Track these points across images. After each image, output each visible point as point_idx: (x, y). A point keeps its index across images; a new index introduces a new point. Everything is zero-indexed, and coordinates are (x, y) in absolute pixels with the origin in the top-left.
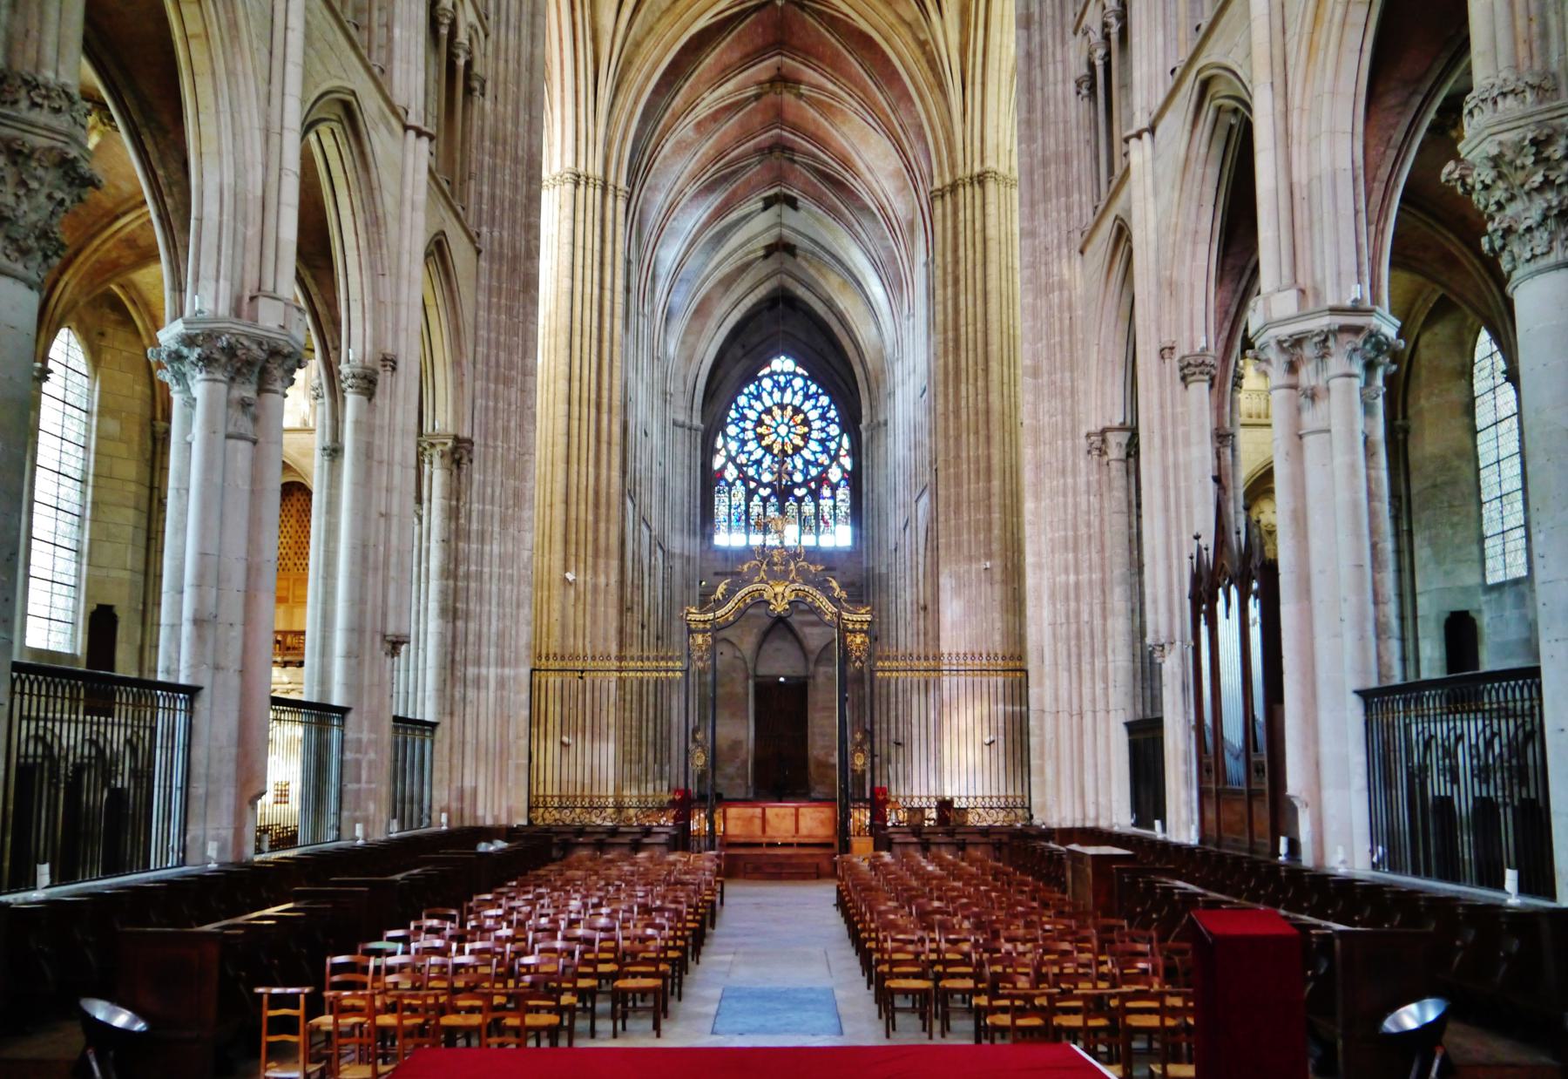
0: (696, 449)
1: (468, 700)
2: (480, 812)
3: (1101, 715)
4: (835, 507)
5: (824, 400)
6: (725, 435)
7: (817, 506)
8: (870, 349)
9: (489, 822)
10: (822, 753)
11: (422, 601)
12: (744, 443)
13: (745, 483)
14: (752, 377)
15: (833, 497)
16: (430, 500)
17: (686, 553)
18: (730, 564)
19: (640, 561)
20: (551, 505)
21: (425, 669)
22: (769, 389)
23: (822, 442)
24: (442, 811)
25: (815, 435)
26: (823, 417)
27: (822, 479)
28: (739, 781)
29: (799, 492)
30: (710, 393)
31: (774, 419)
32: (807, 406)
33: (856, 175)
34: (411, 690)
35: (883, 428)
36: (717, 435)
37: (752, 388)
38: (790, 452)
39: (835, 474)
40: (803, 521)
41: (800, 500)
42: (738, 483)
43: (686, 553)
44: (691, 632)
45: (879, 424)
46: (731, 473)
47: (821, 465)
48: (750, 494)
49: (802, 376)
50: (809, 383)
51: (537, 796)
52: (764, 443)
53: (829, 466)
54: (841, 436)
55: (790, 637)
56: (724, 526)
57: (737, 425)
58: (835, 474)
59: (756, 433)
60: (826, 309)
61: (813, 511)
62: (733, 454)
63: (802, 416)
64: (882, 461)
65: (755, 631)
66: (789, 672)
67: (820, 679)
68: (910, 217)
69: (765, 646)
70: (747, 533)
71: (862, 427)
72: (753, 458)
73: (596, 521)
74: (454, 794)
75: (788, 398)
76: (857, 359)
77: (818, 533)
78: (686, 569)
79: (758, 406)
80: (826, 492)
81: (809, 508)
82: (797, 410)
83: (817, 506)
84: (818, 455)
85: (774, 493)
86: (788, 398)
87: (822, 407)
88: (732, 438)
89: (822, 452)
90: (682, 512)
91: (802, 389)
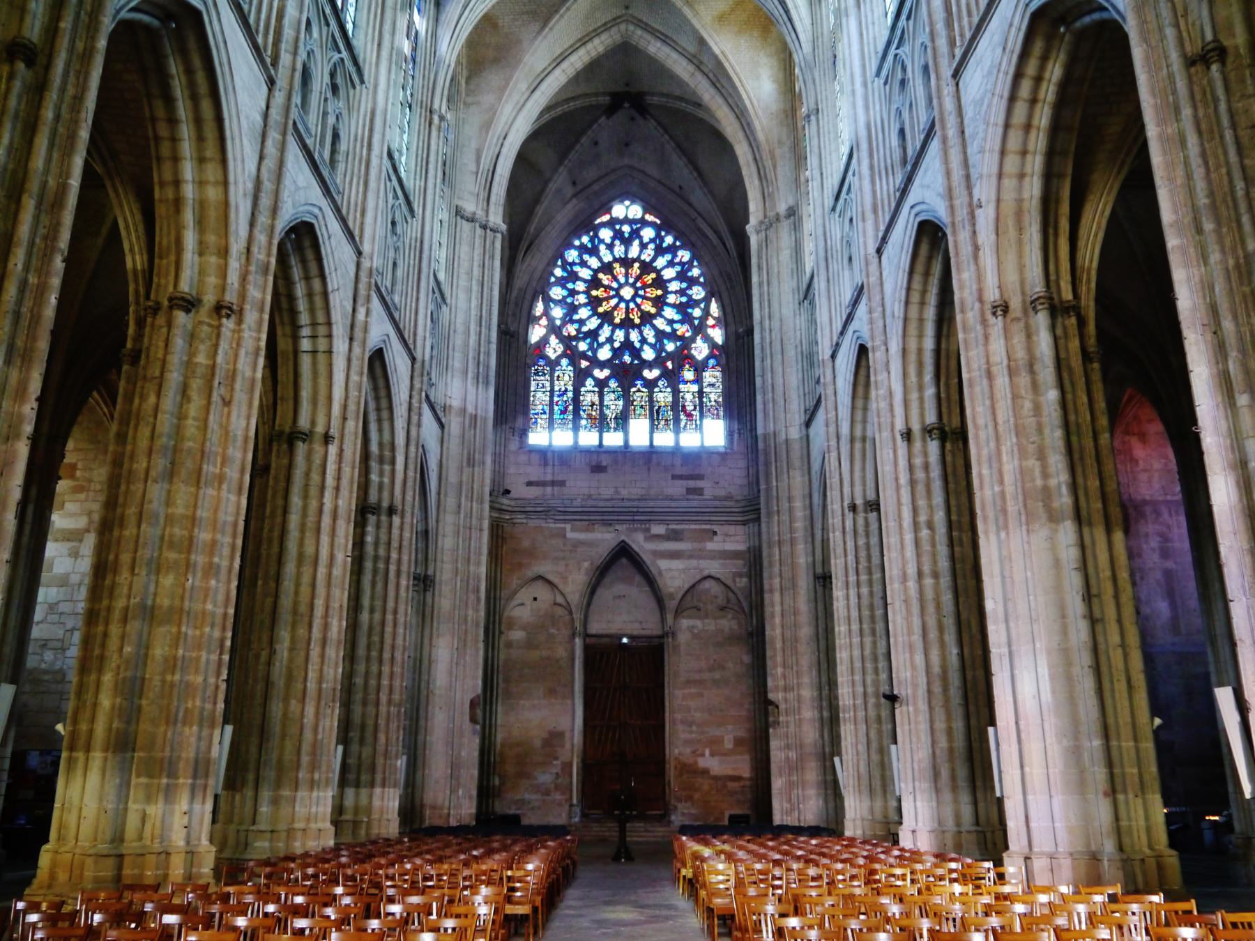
0: (492, 257)
4: (701, 393)
5: (684, 255)
6: (548, 300)
7: (676, 393)
8: (760, 113)
10: (688, 750)
12: (573, 309)
13: (574, 363)
14: (587, 225)
15: (698, 380)
22: (608, 241)
23: (681, 308)
25: (671, 299)
26: (681, 276)
27: (683, 357)
28: (558, 796)
31: (615, 278)
32: (661, 262)
37: (585, 239)
38: (637, 321)
39: (700, 350)
40: (655, 416)
41: (651, 385)
42: (564, 362)
43: (470, 409)
46: (554, 348)
47: (682, 338)
48: (580, 377)
52: (601, 310)
53: (693, 339)
54: (707, 300)
55: (638, 578)
56: (542, 421)
57: (564, 287)
58: (700, 350)
60: (691, 68)
61: (670, 399)
62: (558, 323)
63: (653, 275)
65: (586, 565)
66: (636, 630)
67: (683, 638)
69: (599, 592)
70: (576, 428)
71: (750, 229)
72: (585, 329)
75: (634, 251)
76: (741, 134)
77: (677, 431)
78: (469, 434)
79: (594, 263)
80: (689, 374)
81: (663, 396)
82: (647, 267)
83: (676, 393)
84: (676, 326)
86: (634, 251)
87: (681, 264)
88: (557, 302)
89: (682, 322)
90: (466, 345)
91: (652, 241)
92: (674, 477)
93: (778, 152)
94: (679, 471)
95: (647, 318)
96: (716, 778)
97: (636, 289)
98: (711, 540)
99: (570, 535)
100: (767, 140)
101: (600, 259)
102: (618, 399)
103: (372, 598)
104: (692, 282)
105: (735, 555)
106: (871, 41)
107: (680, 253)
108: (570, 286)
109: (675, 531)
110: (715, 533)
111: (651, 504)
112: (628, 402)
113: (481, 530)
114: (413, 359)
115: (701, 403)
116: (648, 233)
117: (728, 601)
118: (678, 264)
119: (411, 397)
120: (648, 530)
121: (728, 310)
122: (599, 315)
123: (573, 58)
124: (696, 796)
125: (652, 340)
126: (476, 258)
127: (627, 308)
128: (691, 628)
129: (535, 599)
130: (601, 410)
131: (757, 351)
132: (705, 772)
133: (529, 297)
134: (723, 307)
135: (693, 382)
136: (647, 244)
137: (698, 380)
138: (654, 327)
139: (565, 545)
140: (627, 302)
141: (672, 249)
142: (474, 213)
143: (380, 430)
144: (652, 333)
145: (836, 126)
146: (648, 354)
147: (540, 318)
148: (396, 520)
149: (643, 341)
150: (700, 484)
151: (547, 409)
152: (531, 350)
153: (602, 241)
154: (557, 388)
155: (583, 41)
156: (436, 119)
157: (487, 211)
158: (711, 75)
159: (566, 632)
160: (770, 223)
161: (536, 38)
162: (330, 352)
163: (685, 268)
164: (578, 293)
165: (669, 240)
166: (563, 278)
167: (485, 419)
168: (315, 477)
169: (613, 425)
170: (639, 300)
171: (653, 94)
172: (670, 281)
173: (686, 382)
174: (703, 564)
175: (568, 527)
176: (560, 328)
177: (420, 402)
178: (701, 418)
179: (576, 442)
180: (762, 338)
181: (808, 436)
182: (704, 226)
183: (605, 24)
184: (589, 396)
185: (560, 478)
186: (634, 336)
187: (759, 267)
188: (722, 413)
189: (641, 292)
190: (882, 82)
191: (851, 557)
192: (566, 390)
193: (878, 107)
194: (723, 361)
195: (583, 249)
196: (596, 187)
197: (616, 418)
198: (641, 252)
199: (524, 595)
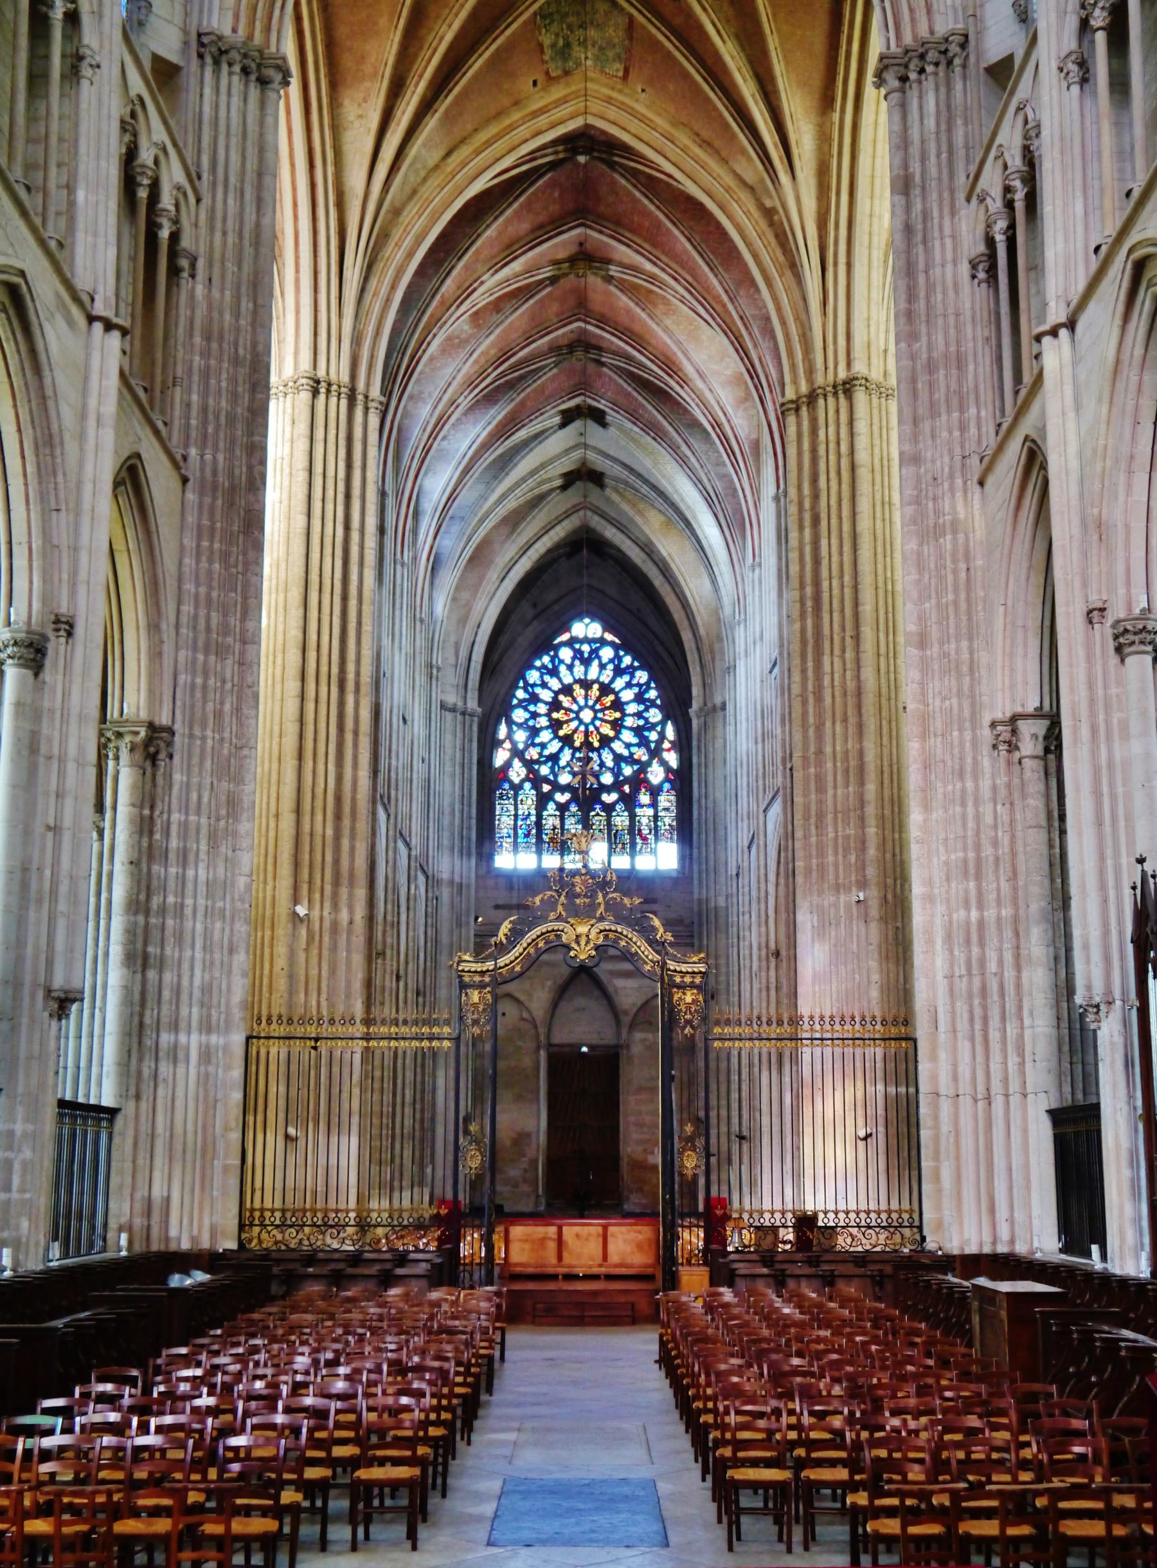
0: (471, 741)
1: (160, 1078)
2: (173, 1232)
3: (1015, 1100)
4: (656, 817)
5: (642, 676)
6: (510, 722)
7: (633, 816)
8: (702, 611)
9: (185, 1245)
10: (640, 1148)
11: (101, 944)
12: (535, 732)
13: (536, 786)
14: (546, 645)
15: (654, 804)
16: (115, 808)
17: (457, 879)
18: (515, 894)
19: (396, 890)
20: (277, 816)
21: (102, 1036)
22: (568, 661)
23: (638, 731)
24: (120, 1229)
25: (629, 722)
26: (639, 698)
27: (639, 781)
28: (525, 1188)
29: (609, 798)
30: (490, 668)
31: (575, 700)
33: (684, 381)
34: (83, 1064)
35: (720, 714)
36: (498, 722)
37: (546, 659)
38: (596, 744)
39: (656, 774)
40: (613, 838)
41: (609, 809)
42: (527, 785)
43: (457, 879)
44: (463, 986)
45: (714, 708)
46: (517, 772)
47: (638, 762)
48: (542, 801)
49: (612, 644)
50: (622, 653)
51: (252, 1210)
52: (561, 733)
53: (649, 763)
54: (663, 723)
55: (596, 992)
56: (507, 844)
57: (525, 709)
58: (656, 774)
59: (550, 719)
60: (643, 555)
61: (627, 823)
62: (521, 746)
63: (612, 697)
64: (719, 758)
65: (549, 983)
66: (595, 1040)
67: (636, 1049)
68: (754, 436)
69: (562, 1004)
71: (692, 712)
72: (546, 752)
73: (337, 837)
74: (138, 1207)
75: (593, 672)
76: (686, 623)
77: (633, 853)
78: (457, 900)
79: (555, 684)
80: (644, 798)
81: (621, 820)
82: (605, 689)
84: (634, 749)
85: (574, 799)
87: (639, 685)
88: (520, 725)
89: (639, 745)
90: (452, 824)
91: (611, 661)
97: (596, 712)
101: (560, 680)
107: (638, 673)
122: (561, 739)
124: (646, 1188)
125: (610, 763)
131: (695, 825)
134: (678, 731)
135: (649, 806)
137: (654, 804)
140: (587, 726)
141: (631, 670)
144: (611, 756)
147: (503, 742)
153: (561, 661)
157: (465, 698)
159: (533, 1045)
161: (505, 541)
163: (643, 689)
166: (525, 700)
167: (468, 886)
170: (598, 723)
172: (627, 703)
173: (642, 806)
180: (700, 814)
182: (660, 649)
184: (551, 820)
189: (600, 715)
196: (556, 608)
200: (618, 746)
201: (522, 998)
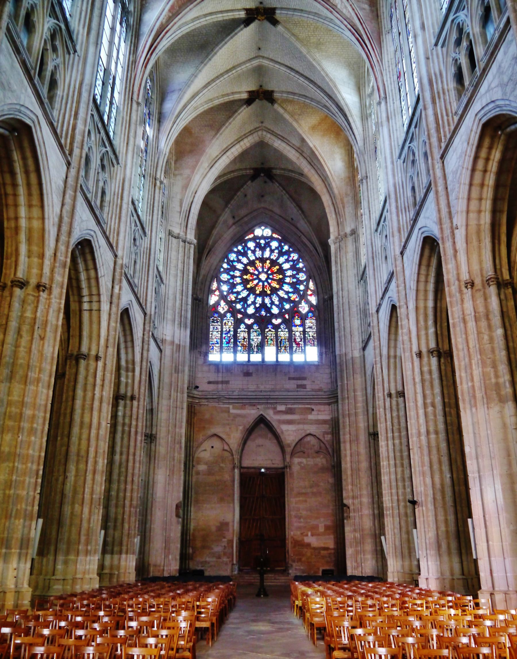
0: (189, 258)
4: (304, 332)
5: (295, 256)
6: (219, 281)
7: (290, 331)
8: (336, 179)
12: (233, 286)
13: (234, 315)
14: (241, 240)
15: (303, 325)
17: (177, 341)
22: (253, 248)
23: (293, 285)
25: (288, 280)
26: (293, 268)
27: (294, 312)
28: (225, 559)
31: (256, 269)
35: (350, 239)
37: (240, 248)
38: (269, 292)
40: (279, 345)
41: (276, 327)
42: (229, 315)
43: (177, 341)
46: (223, 308)
47: (293, 301)
48: (237, 323)
52: (249, 286)
53: (300, 302)
54: (307, 280)
55: (270, 435)
56: (217, 347)
57: (228, 274)
58: (304, 308)
60: (297, 155)
61: (287, 335)
62: (225, 293)
63: (277, 267)
65: (241, 428)
66: (269, 464)
67: (296, 468)
69: (249, 443)
70: (235, 352)
71: (330, 241)
72: (240, 297)
75: (267, 254)
76: (325, 190)
77: (291, 353)
78: (176, 355)
79: (245, 260)
80: (298, 322)
81: (283, 334)
82: (274, 263)
83: (290, 331)
84: (290, 295)
86: (267, 254)
87: (293, 261)
88: (224, 282)
89: (293, 293)
90: (174, 306)
91: (277, 248)
92: (290, 379)
93: (345, 200)
94: (292, 375)
95: (274, 291)
96: (315, 549)
98: (311, 413)
99: (232, 411)
100: (339, 193)
102: (258, 335)
103: (122, 447)
104: (299, 270)
105: (325, 422)
106: (396, 140)
107: (292, 255)
108: (232, 273)
109: (291, 409)
110: (313, 410)
111: (277, 393)
112: (264, 337)
113: (182, 408)
114: (145, 314)
115: (305, 337)
116: (274, 244)
117: (320, 448)
118: (291, 261)
119: (143, 335)
120: (275, 408)
121: (319, 286)
122: (248, 289)
123: (233, 150)
124: (304, 559)
125: (277, 303)
126: (180, 258)
127: (263, 285)
128: (300, 463)
129: (212, 447)
130: (249, 342)
131: (335, 308)
132: (308, 545)
133: (209, 279)
134: (316, 284)
136: (274, 250)
137: (303, 325)
138: (278, 295)
139: (229, 416)
140: (263, 282)
141: (288, 253)
142: (179, 234)
143: (127, 353)
144: (277, 299)
145: (377, 185)
146: (275, 310)
147: (215, 291)
148: (135, 403)
149: (272, 303)
150: (304, 382)
151: (219, 341)
152: (210, 309)
153: (249, 249)
154: (224, 330)
155: (239, 141)
156: (158, 183)
158: (308, 159)
159: (230, 466)
160: (342, 238)
161: (212, 139)
162: (99, 310)
163: (295, 263)
164: (236, 277)
165: (286, 248)
166: (228, 269)
167: (185, 347)
168: (90, 379)
169: (255, 350)
170: (270, 281)
171: (276, 169)
172: (286, 270)
173: (296, 326)
174: (306, 427)
175: (231, 407)
176: (226, 297)
177: (149, 338)
178: (305, 347)
179: (235, 359)
180: (338, 301)
181: (364, 355)
183: (250, 131)
184: (242, 334)
185: (226, 380)
186: (267, 301)
187: (336, 262)
188: (316, 343)
189: (271, 277)
190: (402, 161)
191: (389, 423)
192: (230, 331)
193: (400, 175)
194: (317, 314)
195: (239, 253)
196: (246, 219)
197: (257, 346)
198: (270, 254)
199: (207, 445)
200: (281, 293)
201: (224, 436)
